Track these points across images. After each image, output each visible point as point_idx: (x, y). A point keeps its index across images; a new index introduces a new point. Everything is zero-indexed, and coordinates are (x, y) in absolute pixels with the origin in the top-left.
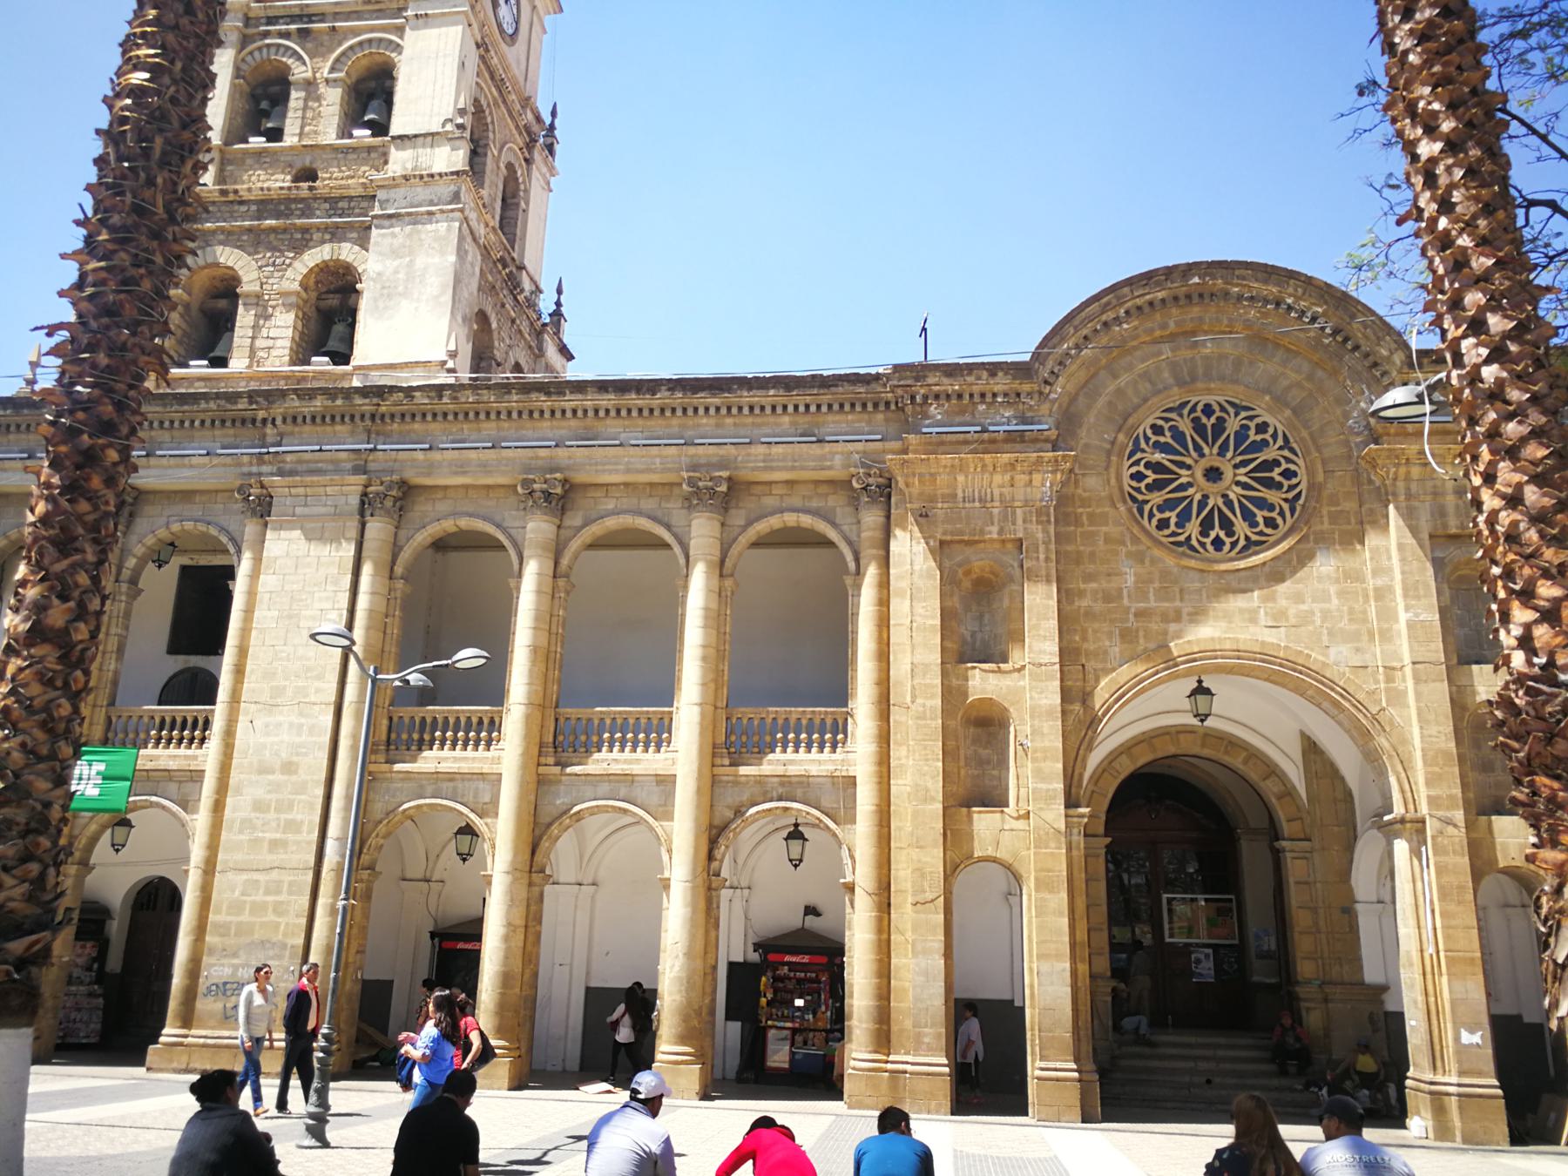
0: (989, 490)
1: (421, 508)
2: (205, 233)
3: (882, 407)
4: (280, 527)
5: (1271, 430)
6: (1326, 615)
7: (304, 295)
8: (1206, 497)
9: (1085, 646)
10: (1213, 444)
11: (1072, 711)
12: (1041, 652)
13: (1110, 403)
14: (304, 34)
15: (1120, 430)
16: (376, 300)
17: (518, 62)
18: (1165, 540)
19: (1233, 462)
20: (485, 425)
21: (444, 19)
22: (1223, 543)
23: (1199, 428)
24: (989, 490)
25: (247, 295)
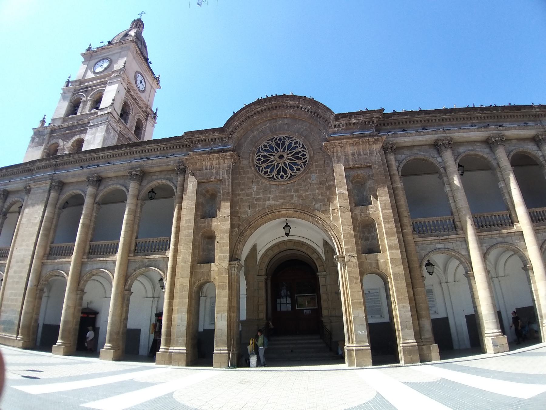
0: (212, 166)
3: (185, 146)
5: (298, 143)
6: (314, 195)
7: (72, 147)
8: (279, 164)
9: (240, 210)
11: (234, 231)
12: (225, 213)
13: (251, 140)
14: (86, 91)
15: (253, 147)
17: (146, 97)
18: (266, 177)
19: (287, 153)
22: (284, 176)
23: (277, 144)
24: (212, 166)
25: (60, 149)
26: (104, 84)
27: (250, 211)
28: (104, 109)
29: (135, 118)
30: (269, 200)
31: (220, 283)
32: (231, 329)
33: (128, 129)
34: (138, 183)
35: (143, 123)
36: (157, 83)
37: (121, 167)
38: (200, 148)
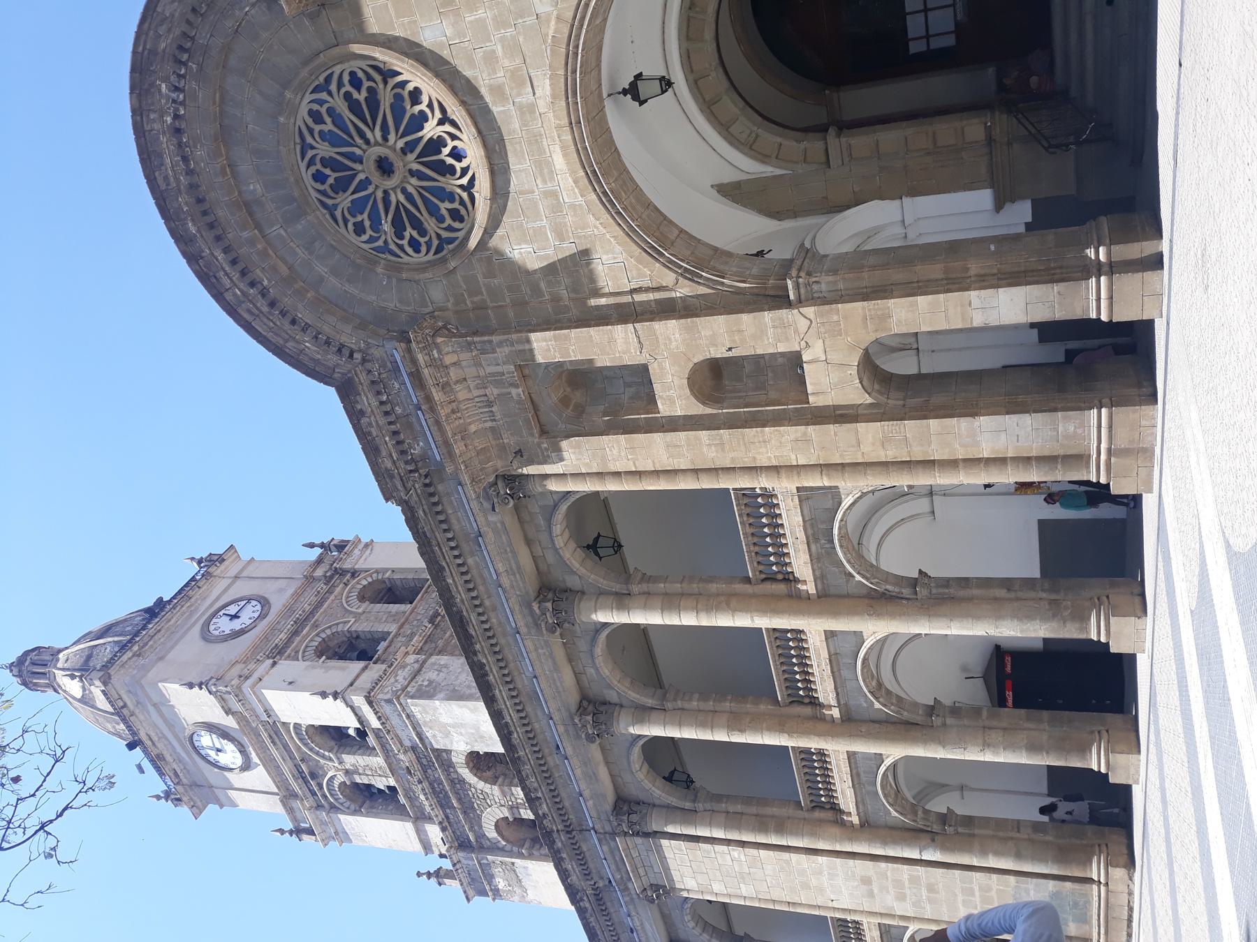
0: (477, 400)
1: (632, 791)
2: (477, 838)
3: (431, 490)
4: (671, 880)
7: (500, 780)
8: (411, 172)
10: (353, 169)
13: (348, 281)
14: (313, 775)
16: (488, 745)
17: (281, 590)
19: (364, 147)
20: (551, 763)
21: (262, 700)
22: (454, 148)
24: (477, 400)
25: (513, 814)
26: (275, 729)
27: (604, 257)
28: (360, 714)
29: (360, 610)
30: (553, 194)
31: (866, 327)
32: (1025, 272)
33: (401, 627)
34: (580, 602)
35: (370, 580)
36: (220, 563)
37: (539, 655)
38: (425, 444)
